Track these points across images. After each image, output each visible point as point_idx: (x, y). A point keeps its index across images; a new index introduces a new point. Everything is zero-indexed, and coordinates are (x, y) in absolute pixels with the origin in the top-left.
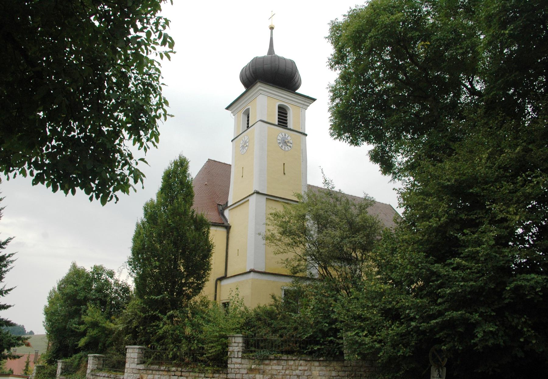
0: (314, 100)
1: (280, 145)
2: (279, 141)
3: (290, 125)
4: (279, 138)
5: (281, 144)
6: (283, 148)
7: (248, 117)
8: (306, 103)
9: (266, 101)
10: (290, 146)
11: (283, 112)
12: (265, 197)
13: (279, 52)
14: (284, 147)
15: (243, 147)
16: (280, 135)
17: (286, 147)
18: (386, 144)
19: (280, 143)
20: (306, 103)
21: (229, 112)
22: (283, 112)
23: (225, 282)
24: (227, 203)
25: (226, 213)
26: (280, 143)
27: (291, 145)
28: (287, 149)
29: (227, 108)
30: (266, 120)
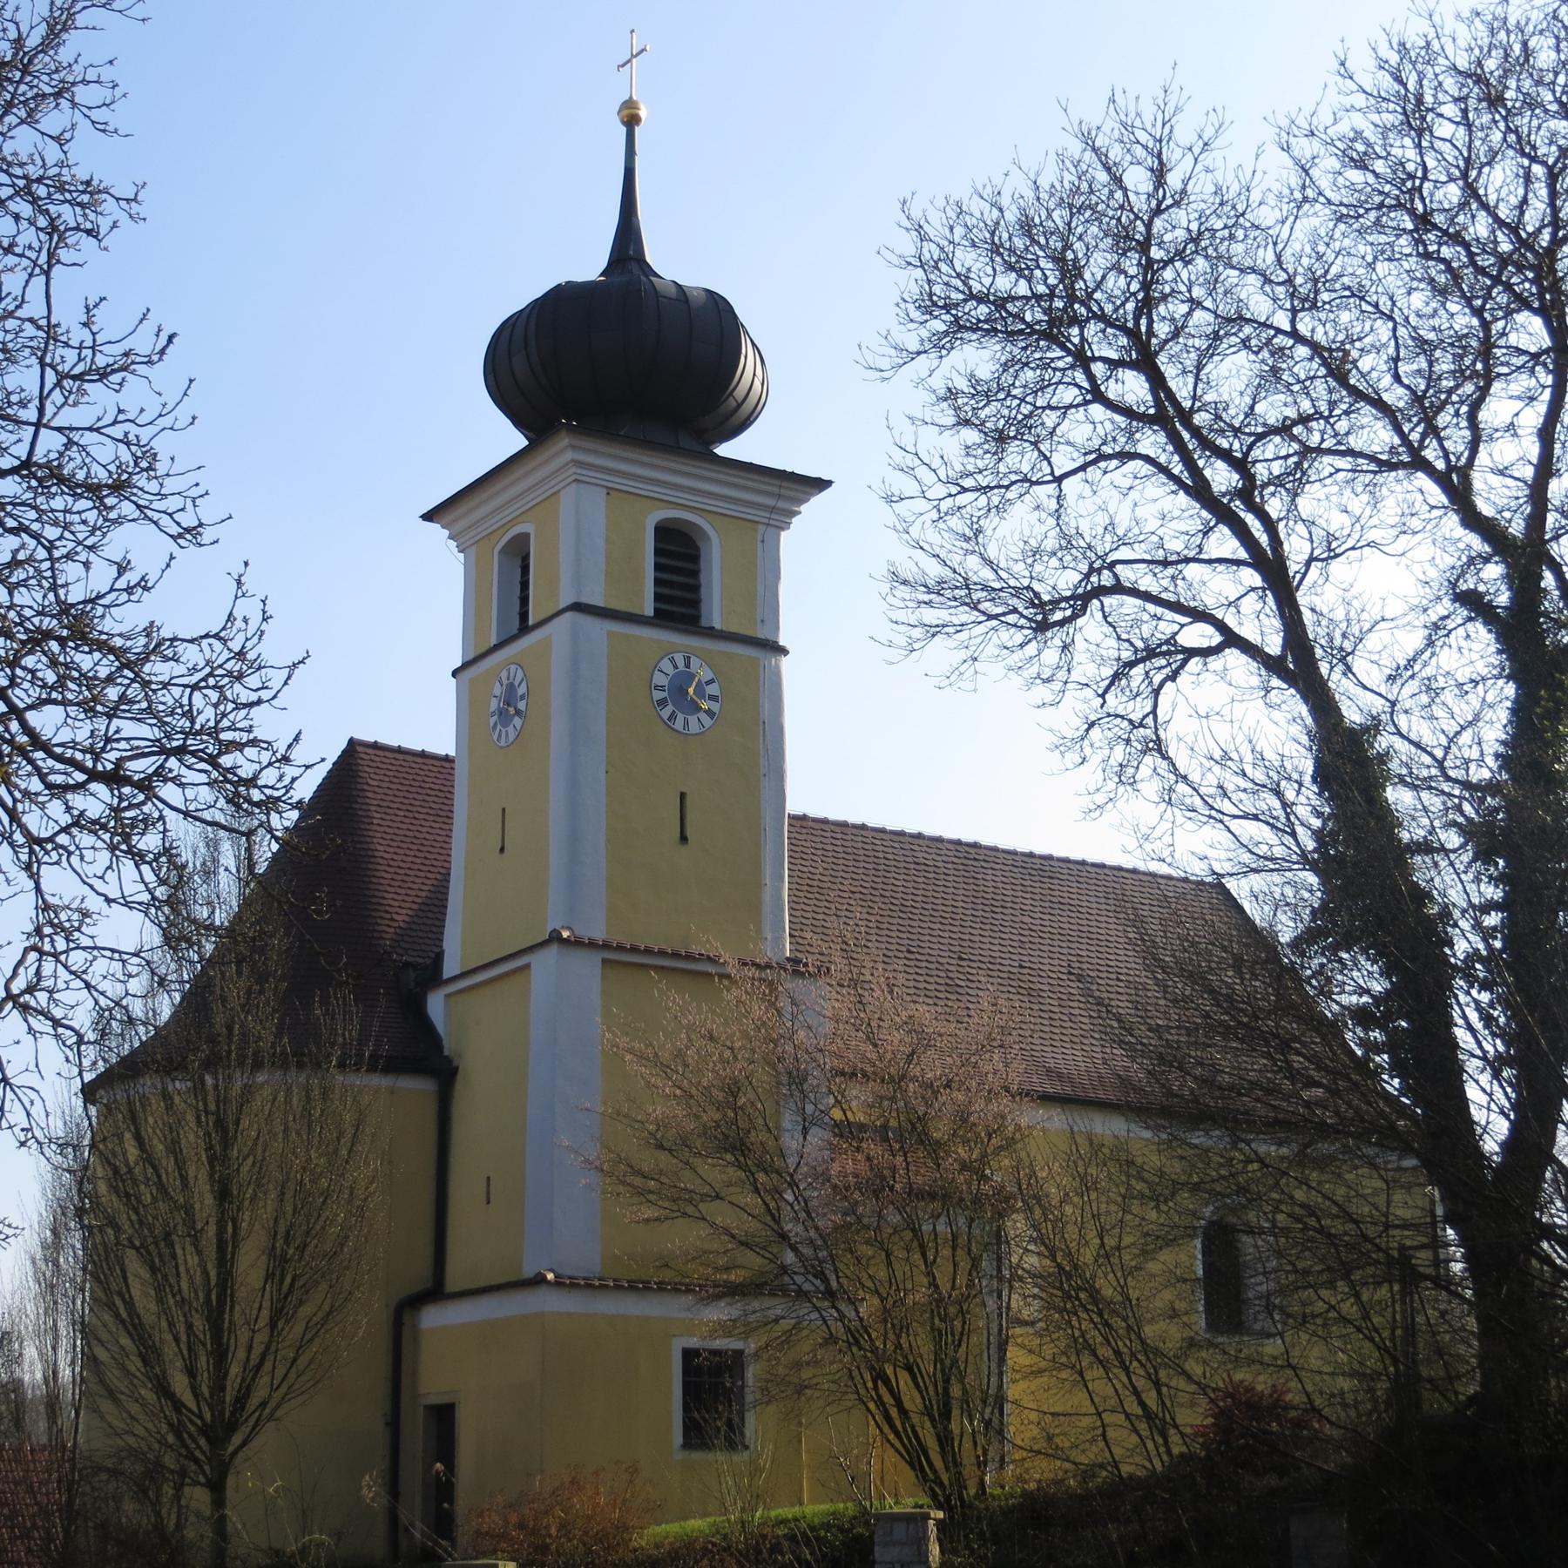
0: (828, 483)
1: (666, 713)
2: (658, 695)
3: (716, 613)
4: (660, 679)
5: (669, 709)
6: (679, 725)
7: (525, 569)
8: (781, 504)
9: (597, 515)
10: (710, 713)
11: (678, 553)
12: (596, 957)
13: (673, 259)
14: (680, 717)
15: (504, 716)
16: (666, 665)
17: (693, 719)
18: (1242, 1041)
19: (662, 703)
20: (781, 504)
21: (436, 531)
22: (678, 553)
23: (433, 1318)
24: (439, 958)
25: (436, 1005)
26: (662, 703)
27: (715, 707)
28: (694, 727)
29: (429, 517)
30: (598, 601)
